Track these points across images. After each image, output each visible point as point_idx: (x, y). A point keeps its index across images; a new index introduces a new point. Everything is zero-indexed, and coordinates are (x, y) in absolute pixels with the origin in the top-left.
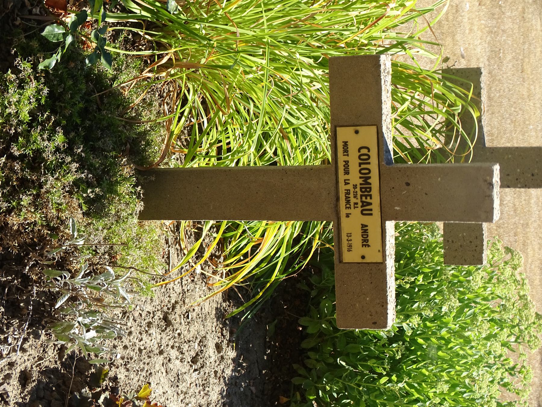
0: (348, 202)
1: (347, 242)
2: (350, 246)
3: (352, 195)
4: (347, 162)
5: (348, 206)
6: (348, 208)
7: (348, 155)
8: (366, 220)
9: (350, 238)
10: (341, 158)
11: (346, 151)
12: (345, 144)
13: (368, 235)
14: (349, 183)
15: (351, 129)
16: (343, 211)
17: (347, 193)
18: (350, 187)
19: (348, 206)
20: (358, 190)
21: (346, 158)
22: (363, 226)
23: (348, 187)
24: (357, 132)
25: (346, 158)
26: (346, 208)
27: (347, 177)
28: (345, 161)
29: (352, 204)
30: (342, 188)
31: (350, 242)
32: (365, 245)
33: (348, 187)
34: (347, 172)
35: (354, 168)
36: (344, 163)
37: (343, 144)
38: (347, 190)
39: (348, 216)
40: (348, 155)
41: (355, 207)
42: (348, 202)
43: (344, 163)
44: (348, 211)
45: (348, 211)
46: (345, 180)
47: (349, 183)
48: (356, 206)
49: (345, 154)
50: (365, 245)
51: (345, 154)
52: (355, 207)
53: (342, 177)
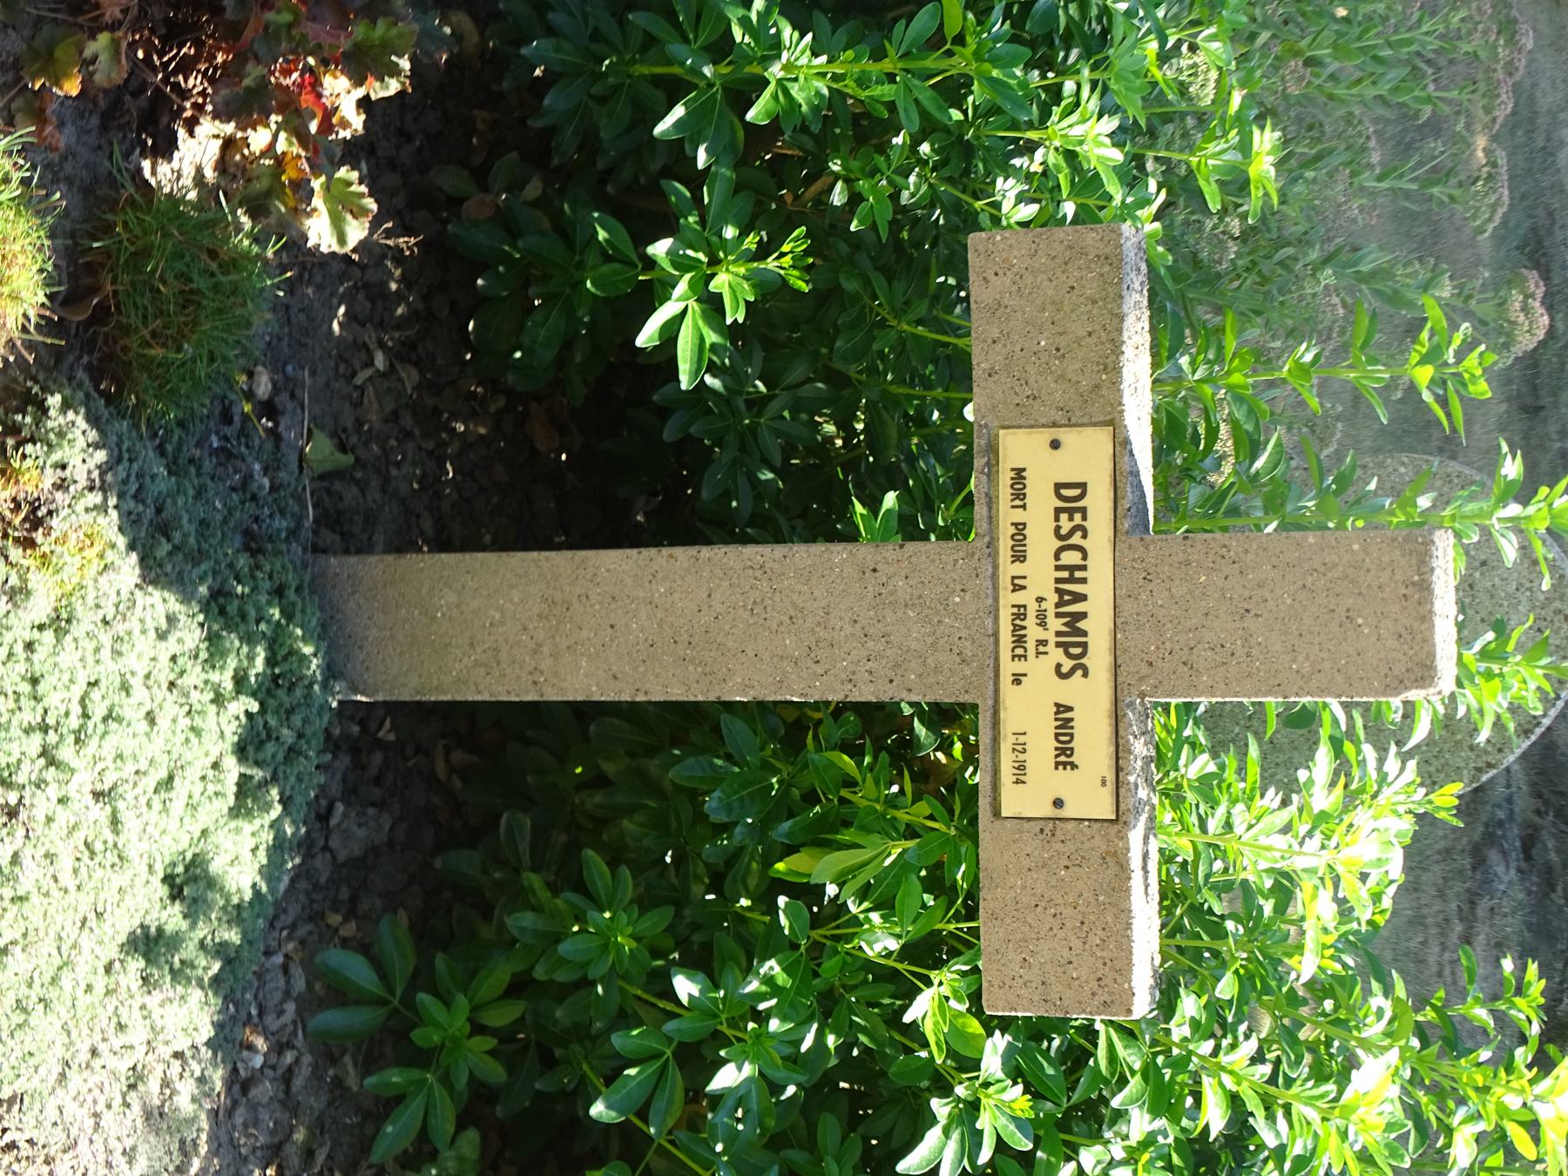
0: (1019, 640)
2: (1021, 767)
3: (1031, 621)
4: (1020, 527)
5: (1019, 651)
6: (1020, 657)
7: (1024, 507)
10: (1007, 515)
11: (1019, 495)
12: (1019, 473)
13: (1072, 735)
14: (1024, 588)
16: (1008, 667)
17: (1017, 616)
19: (1019, 651)
20: (1049, 605)
21: (1018, 515)
23: (1019, 598)
25: (1018, 515)
26: (1013, 657)
27: (1018, 569)
29: (1031, 645)
30: (1008, 599)
31: (1022, 757)
32: (1065, 764)
33: (1019, 598)
34: (1019, 557)
35: (1041, 543)
36: (1012, 530)
37: (1013, 474)
38: (1019, 607)
39: (1017, 680)
40: (1024, 507)
41: (1038, 653)
42: (1019, 640)
43: (1012, 530)
44: (1019, 667)
45: (1019, 667)
46: (1013, 578)
47: (1024, 588)
48: (1041, 649)
49: (1017, 502)
50: (1065, 764)
51: (1017, 502)
52: (1038, 653)
53: (1008, 569)
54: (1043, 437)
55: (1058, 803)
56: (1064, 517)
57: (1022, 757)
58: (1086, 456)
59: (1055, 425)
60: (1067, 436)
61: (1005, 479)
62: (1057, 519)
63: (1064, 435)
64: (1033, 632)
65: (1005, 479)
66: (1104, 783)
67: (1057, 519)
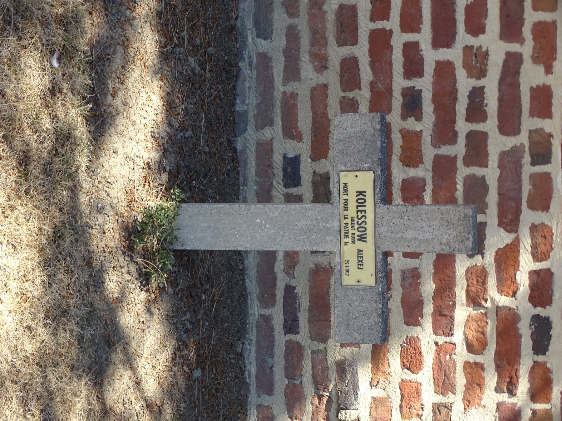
1: (345, 268)
4: (346, 200)
7: (347, 194)
8: (360, 245)
9: (347, 265)
11: (346, 191)
12: (346, 184)
15: (352, 175)
17: (345, 228)
18: (349, 221)
21: (345, 197)
22: (359, 251)
25: (345, 197)
27: (346, 213)
28: (345, 200)
29: (350, 235)
31: (347, 268)
34: (346, 209)
35: (352, 205)
36: (344, 201)
38: (345, 224)
40: (347, 194)
43: (344, 201)
56: (359, 213)
57: (347, 268)
61: (342, 186)
62: (357, 213)
64: (351, 232)
65: (342, 186)
66: (372, 275)
67: (357, 213)
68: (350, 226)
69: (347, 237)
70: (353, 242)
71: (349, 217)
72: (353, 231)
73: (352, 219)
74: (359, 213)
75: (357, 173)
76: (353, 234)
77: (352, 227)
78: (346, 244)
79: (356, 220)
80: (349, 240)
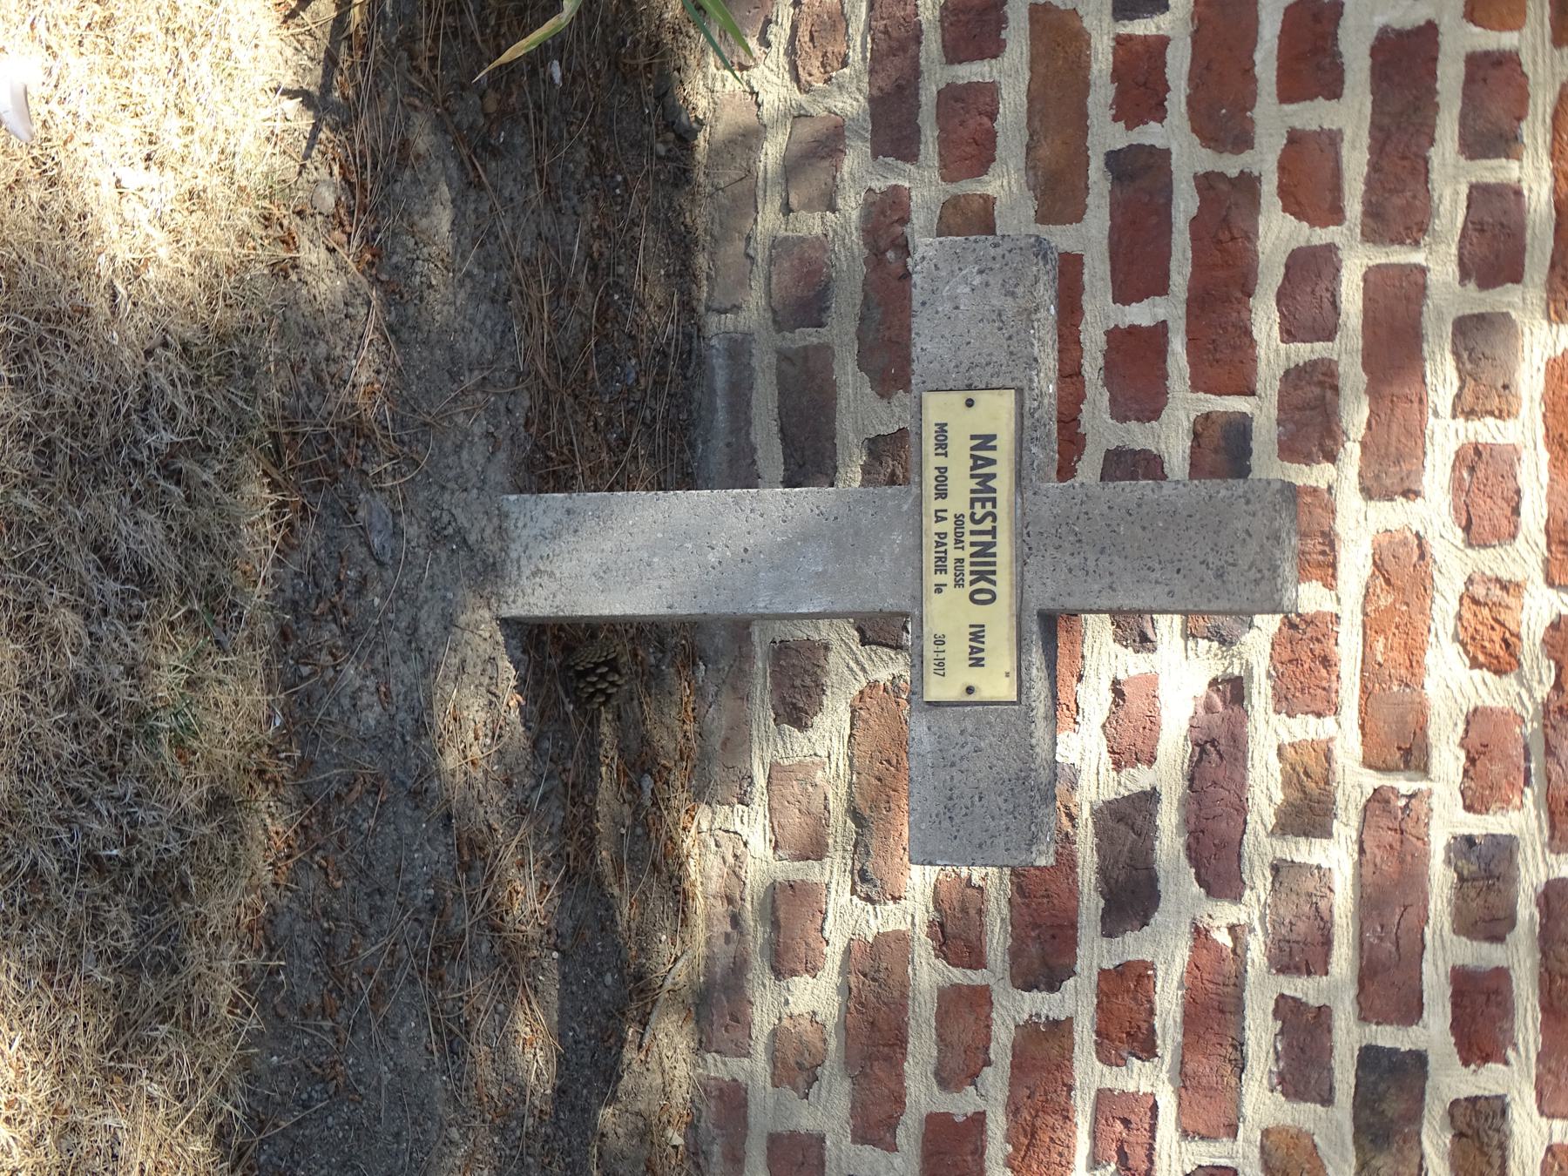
0: (941, 559)
2: (941, 664)
4: (942, 471)
7: (946, 455)
9: (941, 648)
10: (932, 461)
11: (942, 445)
12: (942, 428)
18: (948, 526)
21: (941, 462)
24: (970, 403)
25: (941, 462)
27: (940, 504)
29: (950, 564)
30: (932, 528)
31: (941, 656)
34: (942, 494)
38: (938, 534)
40: (946, 455)
42: (941, 559)
53: (932, 505)
54: (959, 398)
55: (970, 690)
57: (941, 656)
58: (996, 412)
59: (969, 388)
60: (982, 397)
63: (978, 396)
64: (953, 554)
66: (1007, 675)
68: (950, 540)
69: (941, 569)
70: (959, 583)
71: (950, 516)
72: (959, 554)
73: (959, 519)
74: (978, 505)
75: (971, 394)
76: (961, 561)
77: (958, 541)
78: (939, 589)
79: (969, 526)
80: (948, 578)
